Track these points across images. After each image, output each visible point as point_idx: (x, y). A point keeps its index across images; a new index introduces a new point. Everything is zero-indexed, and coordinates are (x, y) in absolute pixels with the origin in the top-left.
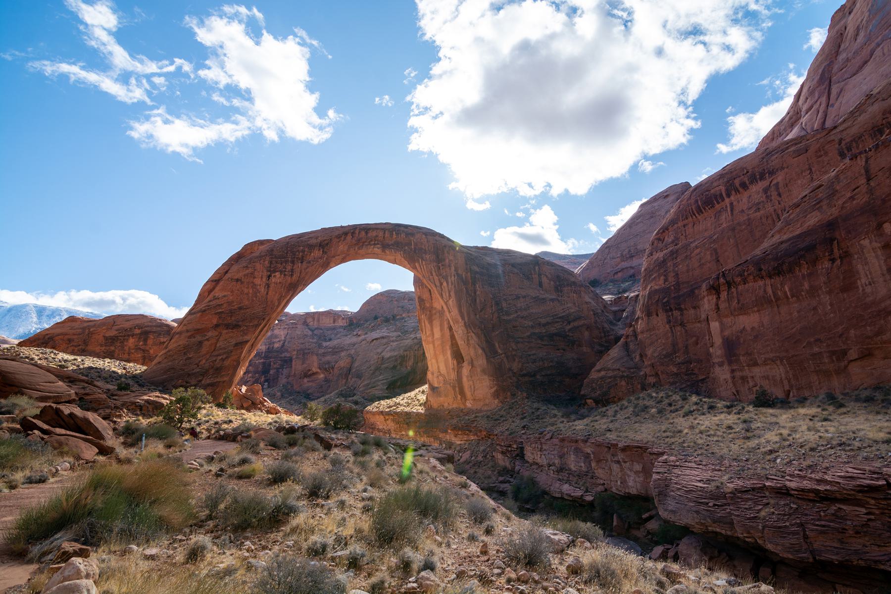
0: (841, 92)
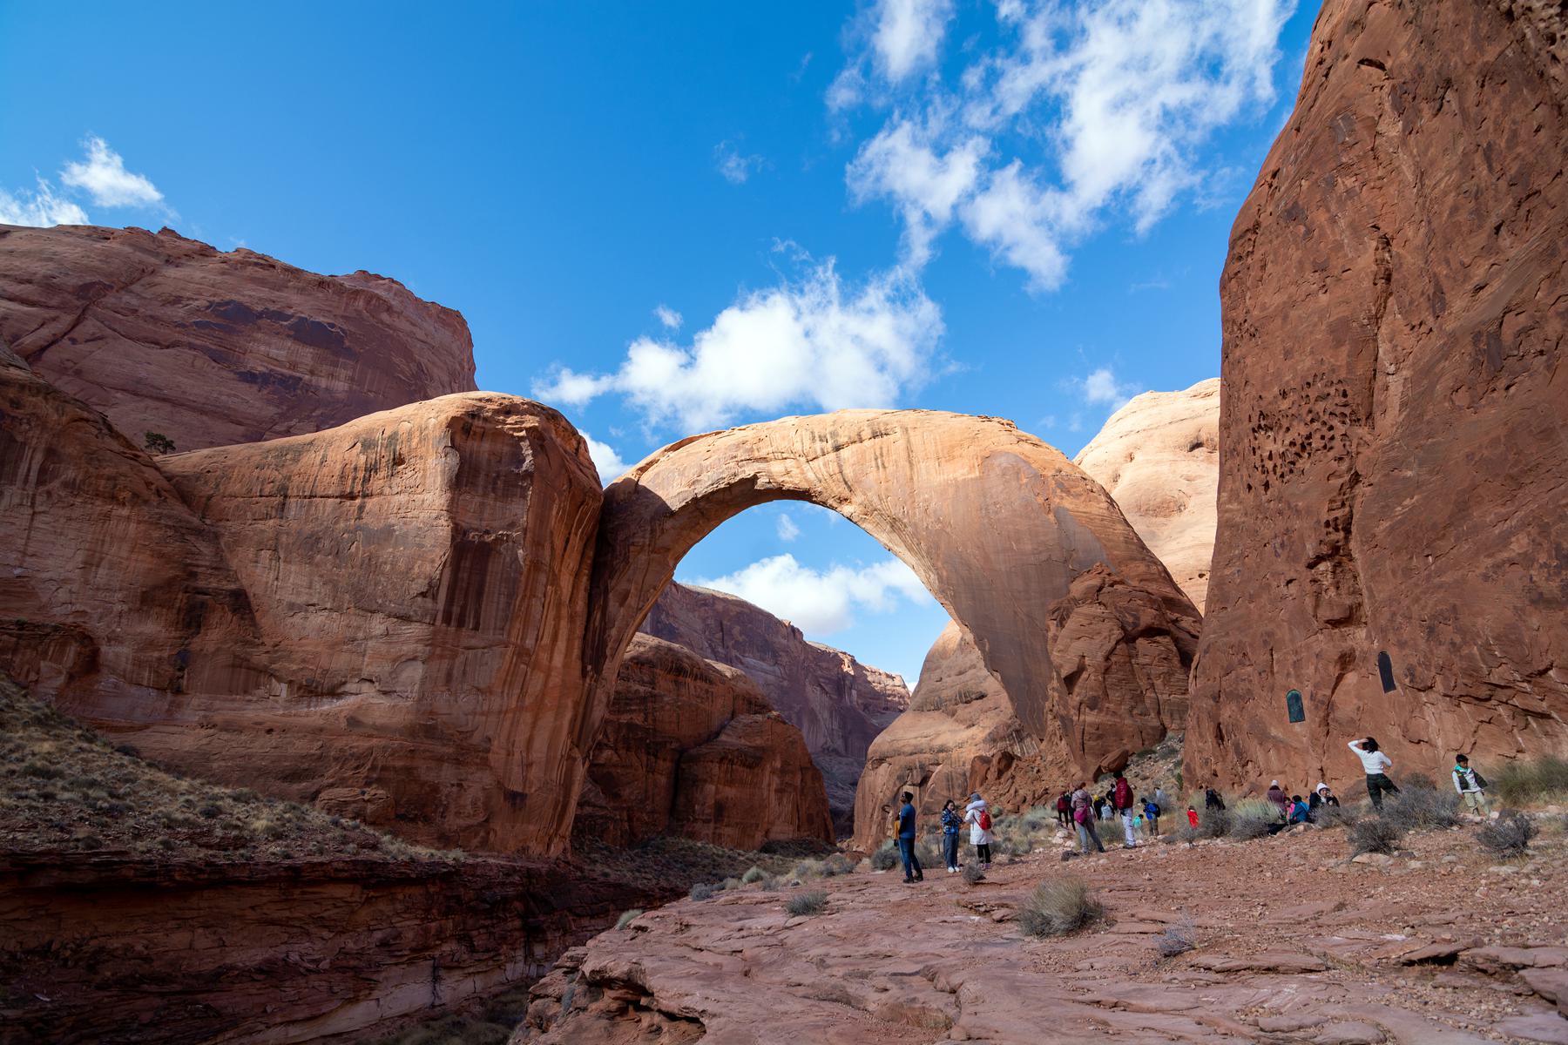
0: (100, 338)
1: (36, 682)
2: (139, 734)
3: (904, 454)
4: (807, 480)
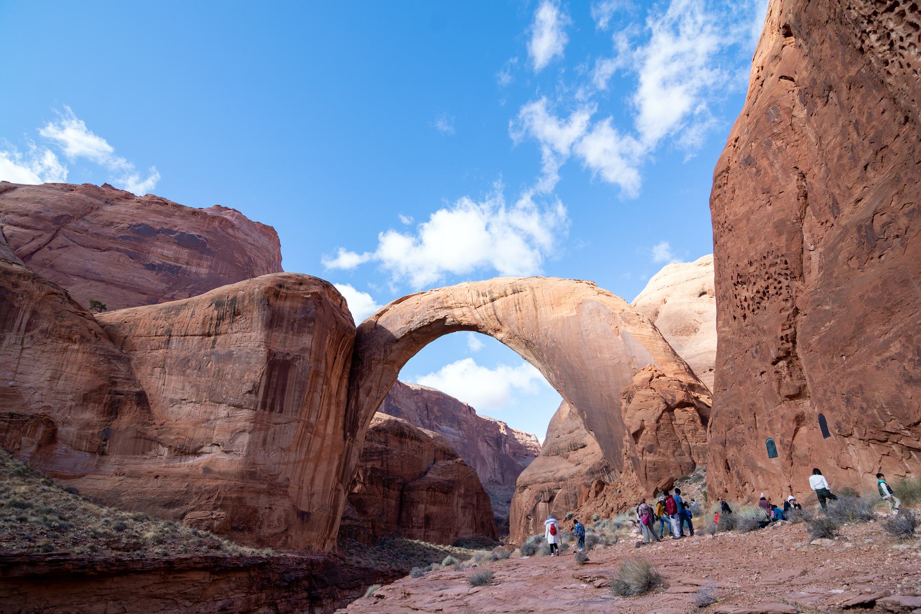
0: (66, 246)
1: (19, 449)
2: (80, 480)
3: (531, 303)
4: (475, 319)
